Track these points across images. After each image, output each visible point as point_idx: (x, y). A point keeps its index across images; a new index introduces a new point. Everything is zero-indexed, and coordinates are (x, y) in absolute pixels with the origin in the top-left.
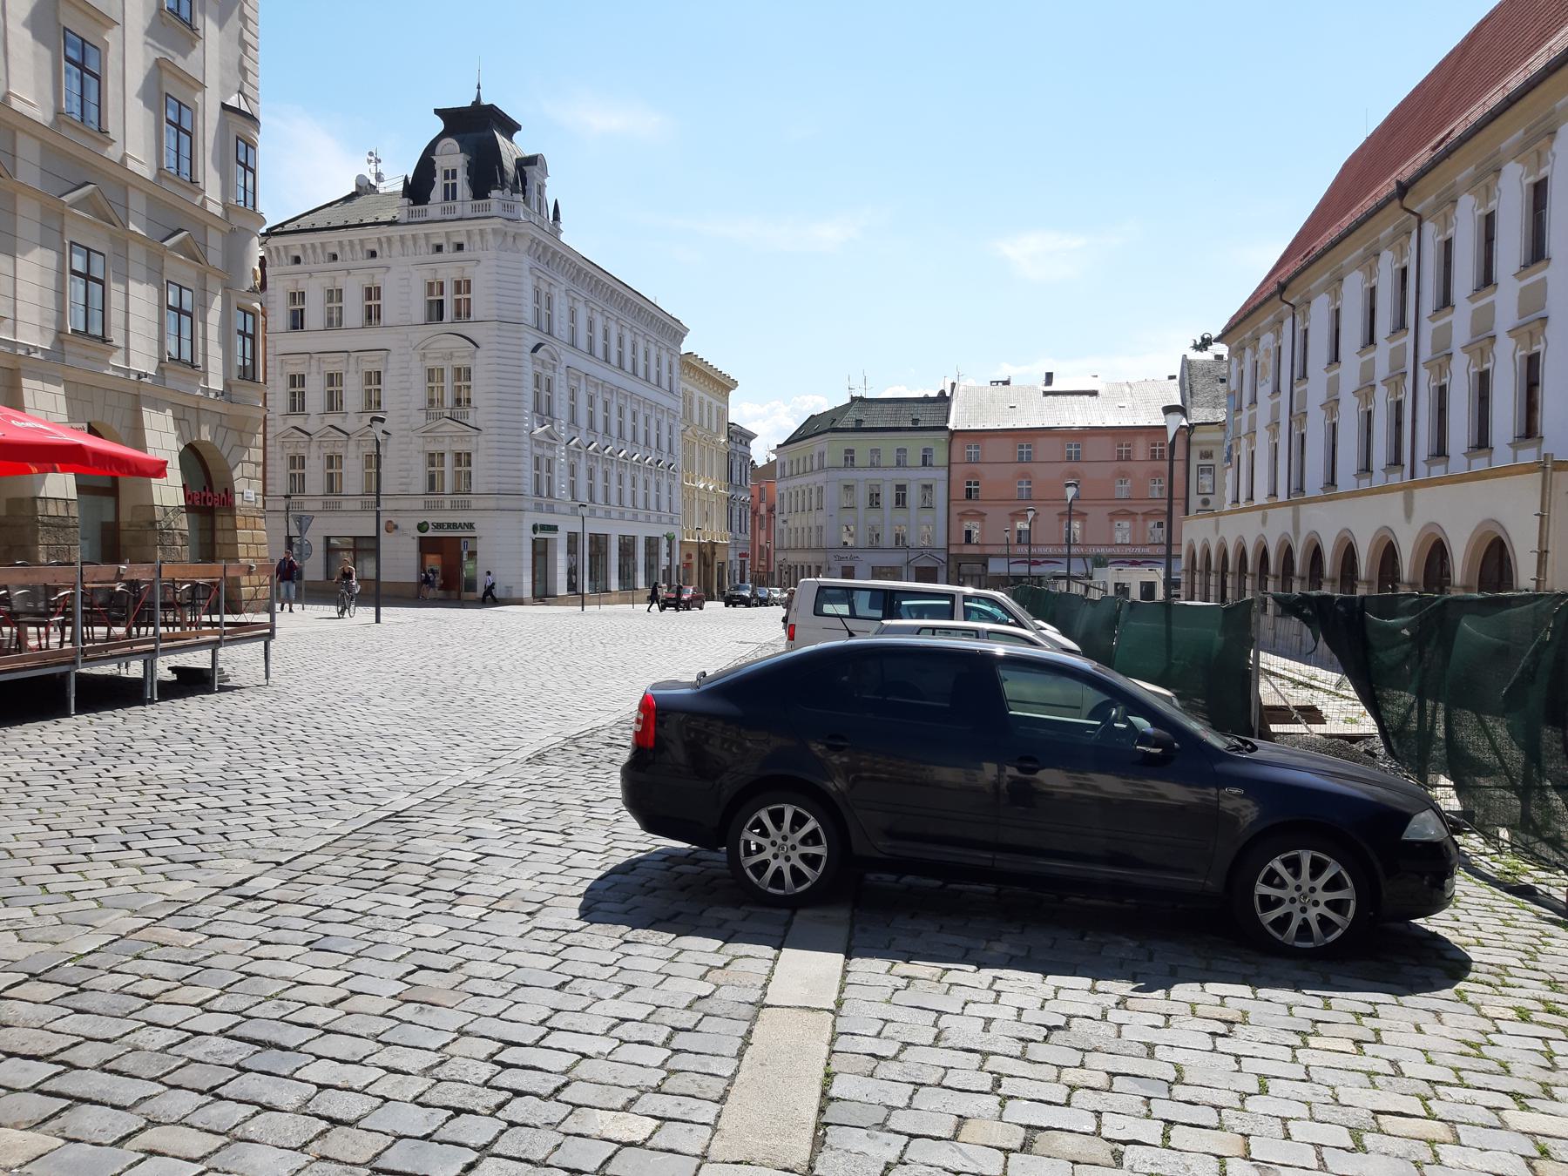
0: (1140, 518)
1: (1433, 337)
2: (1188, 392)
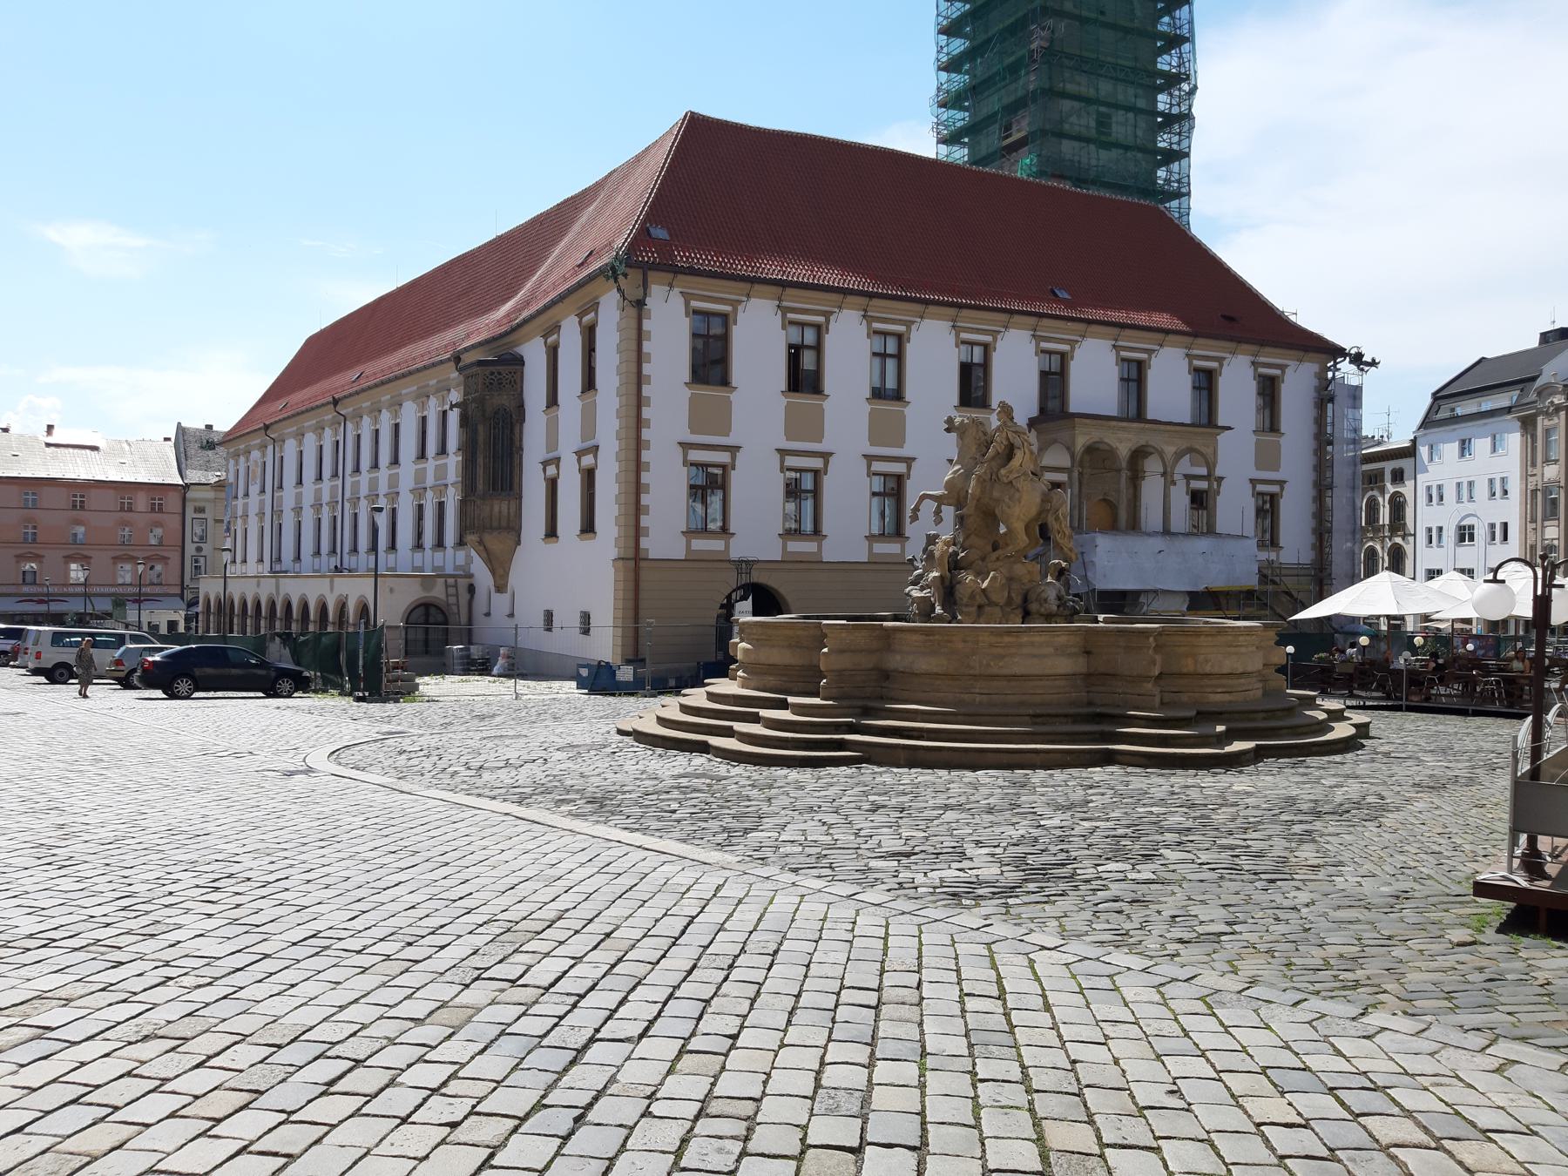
1: (352, 486)
2: (183, 455)
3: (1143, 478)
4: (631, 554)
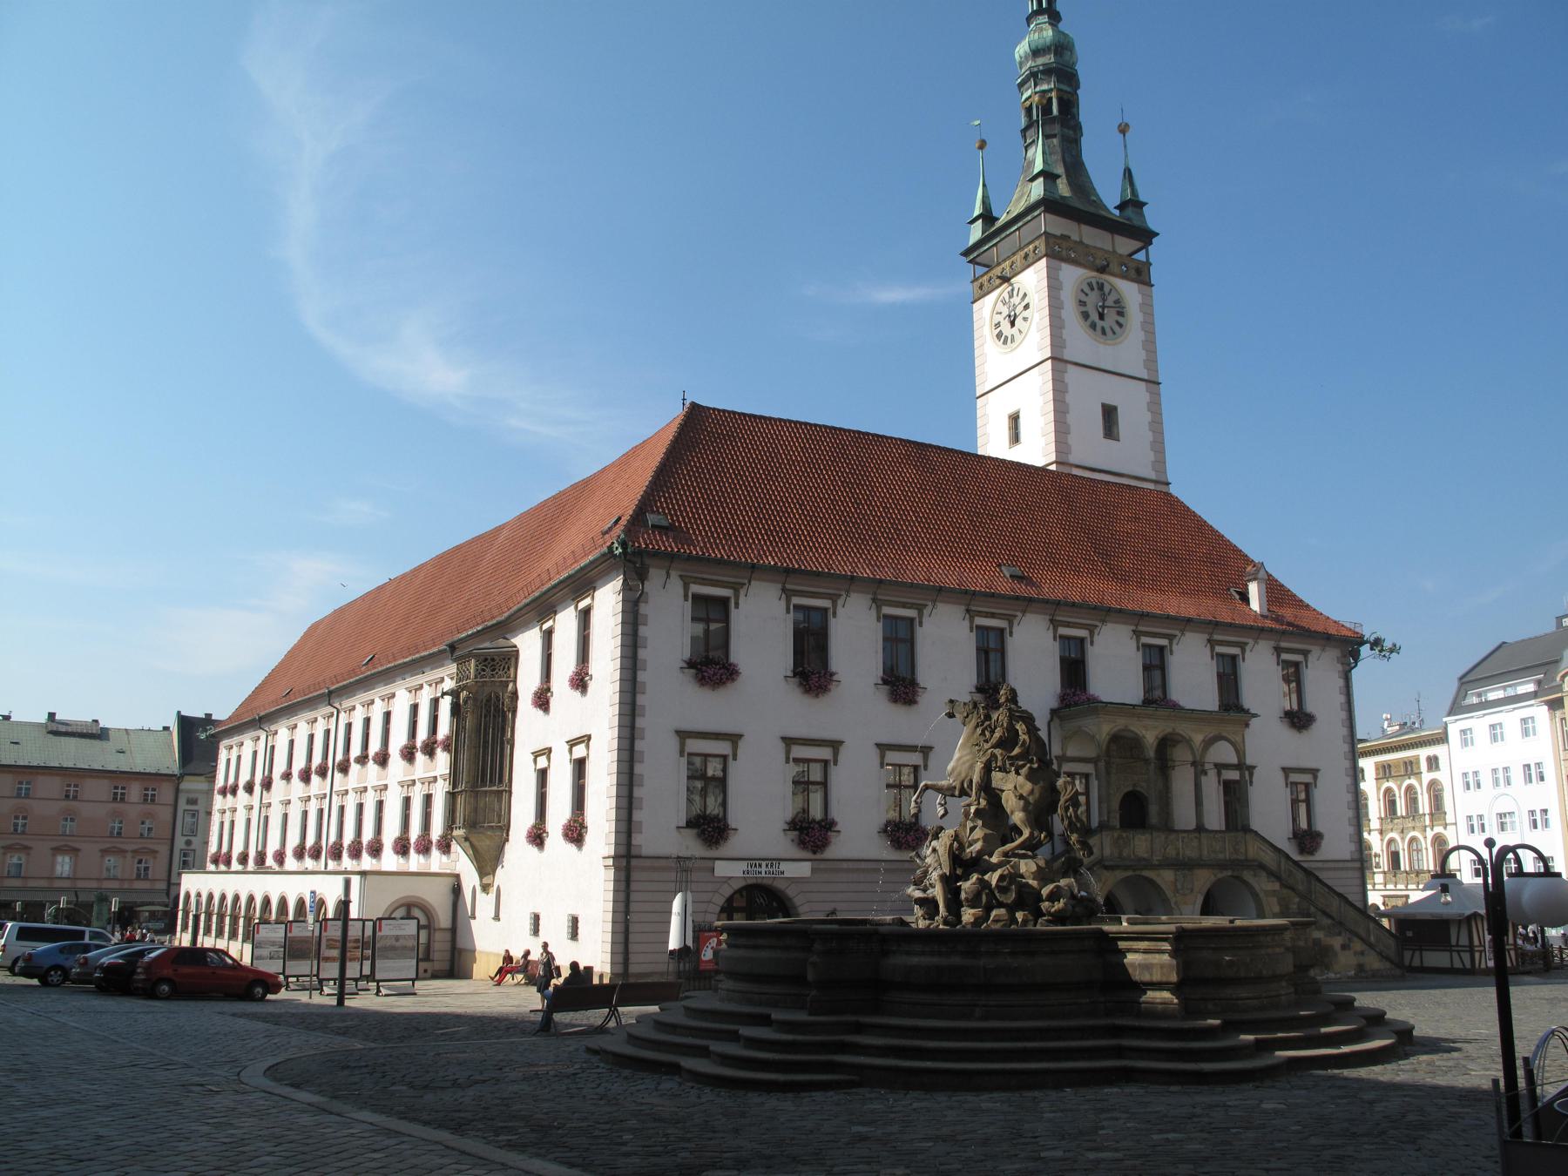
0: (129, 855)
3: (1173, 768)
4: (623, 851)
